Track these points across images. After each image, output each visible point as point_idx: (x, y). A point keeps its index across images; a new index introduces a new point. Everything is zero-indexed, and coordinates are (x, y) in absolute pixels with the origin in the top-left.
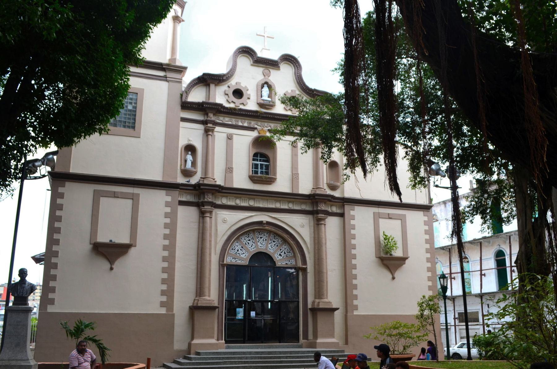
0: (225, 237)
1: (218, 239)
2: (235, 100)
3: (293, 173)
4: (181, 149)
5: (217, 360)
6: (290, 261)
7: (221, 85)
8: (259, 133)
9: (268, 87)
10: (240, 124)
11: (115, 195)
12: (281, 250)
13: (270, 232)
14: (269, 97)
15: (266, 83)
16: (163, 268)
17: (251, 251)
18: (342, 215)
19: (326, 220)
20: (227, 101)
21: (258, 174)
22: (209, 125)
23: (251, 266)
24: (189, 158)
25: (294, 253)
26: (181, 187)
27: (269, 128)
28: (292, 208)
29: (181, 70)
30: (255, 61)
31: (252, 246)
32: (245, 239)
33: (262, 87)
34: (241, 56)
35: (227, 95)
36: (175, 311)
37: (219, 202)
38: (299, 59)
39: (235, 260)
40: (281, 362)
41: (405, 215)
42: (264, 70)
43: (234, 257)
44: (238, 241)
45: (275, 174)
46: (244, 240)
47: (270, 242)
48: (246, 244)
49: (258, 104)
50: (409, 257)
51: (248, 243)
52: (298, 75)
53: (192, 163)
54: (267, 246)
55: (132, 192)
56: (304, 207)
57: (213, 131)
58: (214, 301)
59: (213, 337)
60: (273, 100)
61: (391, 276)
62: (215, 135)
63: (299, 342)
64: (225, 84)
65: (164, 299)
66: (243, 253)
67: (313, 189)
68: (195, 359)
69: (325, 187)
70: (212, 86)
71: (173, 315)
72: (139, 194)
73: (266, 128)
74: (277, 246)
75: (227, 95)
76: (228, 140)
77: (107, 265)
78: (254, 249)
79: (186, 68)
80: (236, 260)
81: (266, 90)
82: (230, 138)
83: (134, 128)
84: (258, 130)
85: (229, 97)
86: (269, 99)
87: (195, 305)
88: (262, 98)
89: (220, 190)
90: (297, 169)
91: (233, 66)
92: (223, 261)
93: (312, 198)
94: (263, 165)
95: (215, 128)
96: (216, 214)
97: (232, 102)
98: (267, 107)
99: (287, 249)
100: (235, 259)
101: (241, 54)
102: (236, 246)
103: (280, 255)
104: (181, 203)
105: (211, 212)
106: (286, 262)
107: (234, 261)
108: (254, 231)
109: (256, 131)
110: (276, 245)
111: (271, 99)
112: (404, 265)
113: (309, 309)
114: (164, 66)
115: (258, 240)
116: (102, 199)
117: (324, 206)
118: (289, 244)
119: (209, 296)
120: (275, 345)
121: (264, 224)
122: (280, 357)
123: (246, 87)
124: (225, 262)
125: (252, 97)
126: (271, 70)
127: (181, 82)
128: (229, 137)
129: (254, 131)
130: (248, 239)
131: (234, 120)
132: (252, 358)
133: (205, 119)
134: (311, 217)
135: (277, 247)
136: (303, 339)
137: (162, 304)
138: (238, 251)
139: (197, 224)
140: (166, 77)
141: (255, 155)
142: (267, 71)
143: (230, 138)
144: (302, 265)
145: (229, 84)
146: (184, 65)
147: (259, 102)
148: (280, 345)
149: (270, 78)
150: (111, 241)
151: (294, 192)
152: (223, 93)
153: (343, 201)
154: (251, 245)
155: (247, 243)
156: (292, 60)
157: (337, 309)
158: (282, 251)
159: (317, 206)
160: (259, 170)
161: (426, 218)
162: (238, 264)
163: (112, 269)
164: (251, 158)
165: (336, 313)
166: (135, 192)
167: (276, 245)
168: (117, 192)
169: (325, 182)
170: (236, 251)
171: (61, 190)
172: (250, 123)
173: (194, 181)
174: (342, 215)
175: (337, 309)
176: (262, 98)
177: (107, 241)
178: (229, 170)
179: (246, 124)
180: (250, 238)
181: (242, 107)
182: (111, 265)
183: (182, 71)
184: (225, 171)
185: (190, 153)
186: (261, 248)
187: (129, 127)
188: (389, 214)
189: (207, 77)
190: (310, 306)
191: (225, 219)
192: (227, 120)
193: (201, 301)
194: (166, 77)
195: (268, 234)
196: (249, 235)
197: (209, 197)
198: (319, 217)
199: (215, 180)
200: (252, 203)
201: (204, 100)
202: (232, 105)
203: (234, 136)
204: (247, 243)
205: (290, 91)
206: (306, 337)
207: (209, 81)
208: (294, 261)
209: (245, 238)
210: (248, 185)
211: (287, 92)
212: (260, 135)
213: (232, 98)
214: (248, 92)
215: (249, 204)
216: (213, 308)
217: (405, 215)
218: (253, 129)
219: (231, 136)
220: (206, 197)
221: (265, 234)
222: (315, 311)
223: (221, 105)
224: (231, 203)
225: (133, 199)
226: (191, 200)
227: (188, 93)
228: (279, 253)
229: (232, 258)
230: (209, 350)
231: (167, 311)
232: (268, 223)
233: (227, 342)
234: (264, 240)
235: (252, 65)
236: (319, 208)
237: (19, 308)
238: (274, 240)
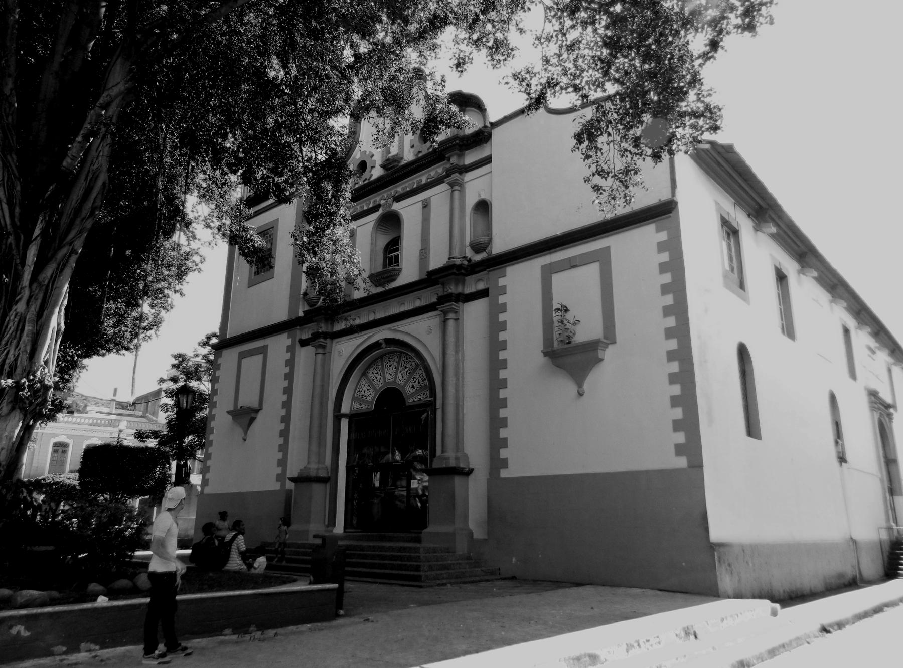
103: (413, 387)
106: (420, 397)
161: (663, 236)
228: (411, 384)
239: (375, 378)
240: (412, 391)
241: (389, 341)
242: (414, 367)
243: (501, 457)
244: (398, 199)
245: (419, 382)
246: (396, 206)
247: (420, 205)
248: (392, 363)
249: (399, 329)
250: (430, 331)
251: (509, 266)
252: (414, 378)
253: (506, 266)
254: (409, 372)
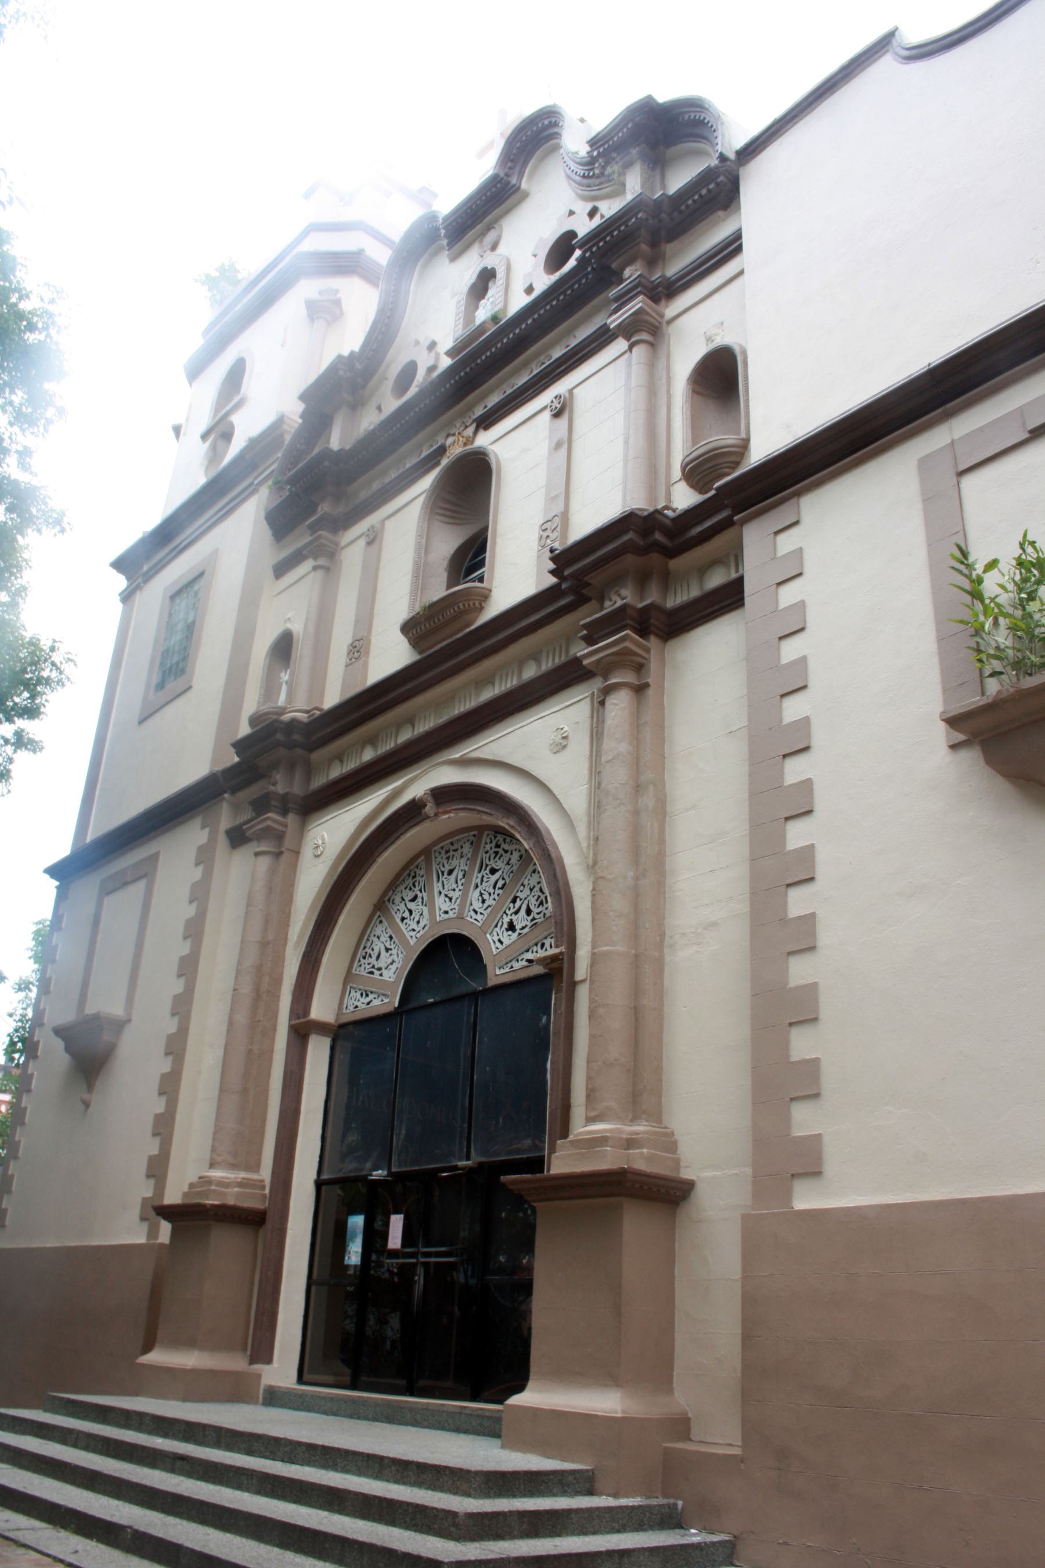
31: (418, 922)
39: (368, 1000)
51: (411, 912)
80: (371, 997)
103: (511, 927)
186: (446, 916)
228: (506, 920)
235: (453, 259)
239: (407, 914)
240: (509, 938)
241: (444, 795)
242: (515, 868)
244: (486, 422)
245: (529, 912)
246: (484, 440)
247: (547, 415)
248: (454, 863)
249: (474, 755)
250: (561, 745)
251: (809, 489)
252: (514, 901)
253: (799, 494)
254: (499, 885)
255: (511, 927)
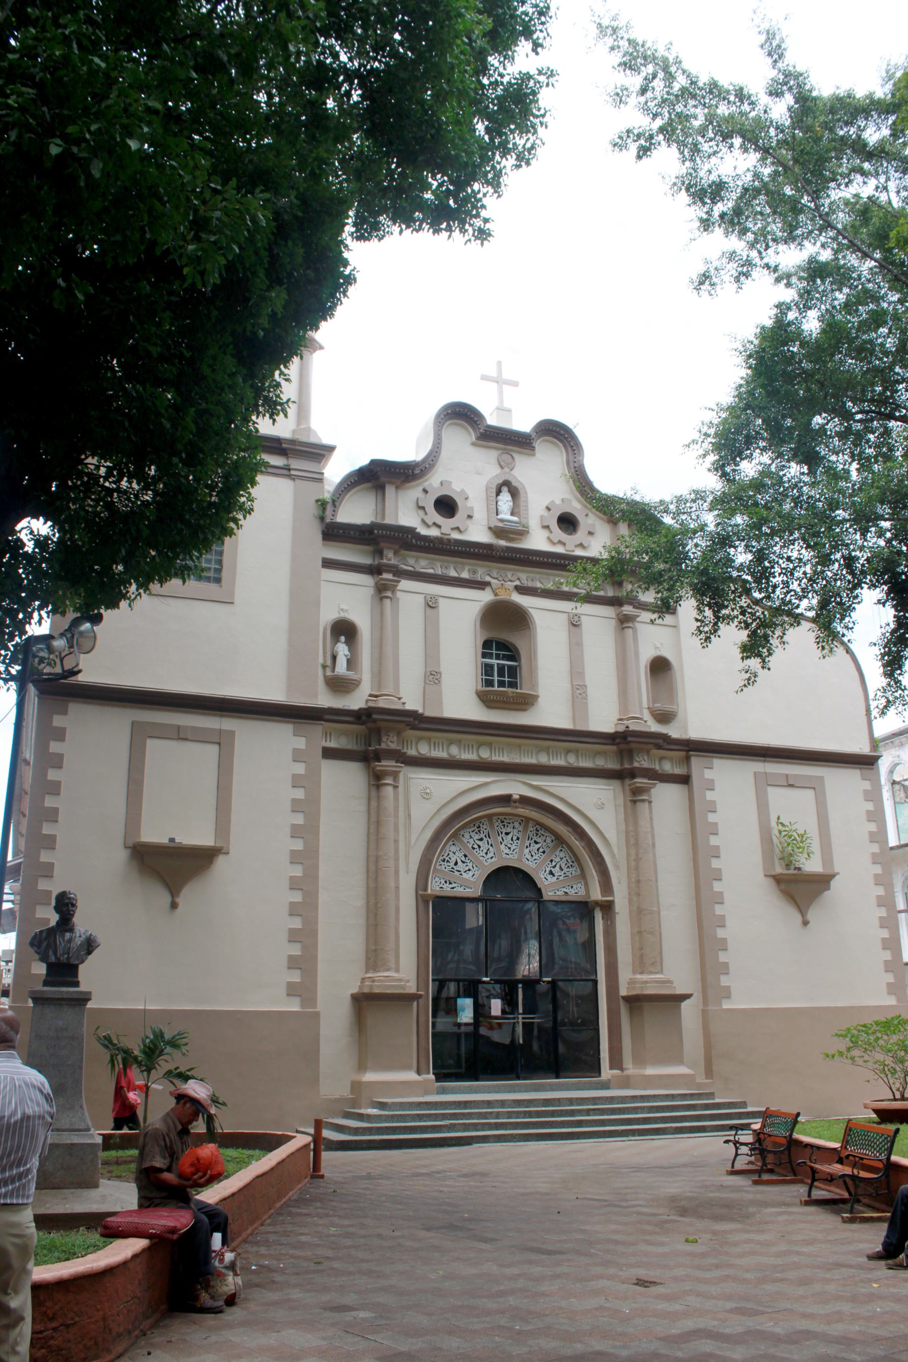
0: (429, 834)
1: (414, 838)
2: (440, 520)
3: (575, 683)
4: (325, 629)
5: (430, 1121)
6: (575, 887)
7: (409, 488)
8: (496, 595)
9: (509, 491)
10: (453, 573)
11: (180, 735)
12: (551, 861)
13: (526, 821)
14: (512, 514)
15: (506, 483)
16: (292, 904)
17: (486, 864)
18: (685, 780)
19: (652, 790)
20: (423, 522)
21: (493, 686)
22: (386, 576)
23: (486, 900)
24: (342, 649)
25: (582, 870)
26: (326, 717)
27: (517, 583)
28: (576, 764)
29: (320, 453)
30: (481, 434)
31: (486, 853)
32: (471, 837)
33: (498, 492)
34: (450, 424)
35: (423, 508)
36: (321, 1006)
37: (412, 752)
38: (578, 432)
40: (579, 1124)
41: (823, 777)
42: (501, 455)
43: (447, 879)
44: (456, 842)
45: (534, 685)
46: (470, 838)
47: (527, 843)
48: (474, 848)
49: (490, 528)
50: (838, 874)
51: (479, 847)
52: (576, 465)
53: (348, 661)
54: (521, 853)
55: (217, 726)
56: (601, 763)
57: (393, 589)
58: (408, 981)
59: (406, 1067)
60: (524, 521)
61: (799, 918)
62: (398, 599)
63: (600, 1075)
64: (418, 485)
65: (296, 977)
66: (467, 868)
67: (621, 720)
68: (379, 1118)
69: (647, 716)
70: (390, 491)
71: (317, 1015)
72: (232, 733)
73: (509, 583)
74: (544, 852)
75: (423, 508)
76: (428, 609)
77: (166, 899)
78: (493, 860)
79: (331, 449)
81: (505, 499)
82: (431, 605)
83: (218, 580)
84: (494, 587)
85: (426, 514)
86: (515, 519)
87: (366, 990)
88: (500, 517)
89: (417, 722)
90: (582, 674)
91: (434, 445)
92: (426, 889)
93: (618, 741)
94: (503, 666)
95: (399, 582)
96: (407, 780)
97: (435, 524)
98: (511, 536)
99: (564, 859)
100: (450, 883)
101: (450, 419)
102: (451, 853)
103: (551, 873)
104: (329, 754)
105: (395, 775)
106: (565, 890)
107: (447, 887)
108: (490, 817)
109: (488, 589)
110: (541, 850)
111: (519, 518)
112: (827, 893)
113: (623, 998)
114: (284, 445)
115: (500, 839)
116: (151, 744)
117: (646, 758)
118: (570, 848)
119: (397, 970)
120: (550, 1084)
121: (515, 802)
122: (572, 1113)
123: (463, 491)
124: (429, 891)
125: (476, 516)
126: (515, 455)
127: (320, 480)
128: (430, 604)
129: (483, 589)
130: (477, 837)
131: (439, 564)
132: (510, 1115)
133: (376, 562)
134: (615, 785)
135: (544, 856)
136: (611, 1068)
137: (292, 990)
138: (456, 864)
139: (364, 802)
140: (289, 470)
141: (487, 644)
142: (506, 457)
143: (431, 605)
144: (603, 896)
145: (426, 485)
146: (326, 440)
147: (493, 526)
148: (559, 1083)
149: (515, 472)
150: (172, 840)
151: (578, 728)
152: (414, 505)
153: (687, 748)
154: (485, 851)
155: (476, 846)
156: (561, 435)
157: (687, 996)
158: (554, 864)
159: (631, 760)
160: (496, 678)
161: (867, 785)
162: (458, 895)
163: (174, 906)
164: (480, 651)
165: (685, 1005)
166: (224, 727)
167: (541, 850)
168: (186, 727)
169: (645, 705)
170: (452, 864)
171: (58, 721)
172: (475, 572)
173: (356, 701)
174: (685, 780)
175: (687, 996)
176: (500, 517)
177: (164, 840)
178: (433, 677)
179: (465, 575)
180: (482, 836)
181: (455, 536)
182: (173, 896)
183: (323, 456)
184: (423, 679)
185: (343, 638)
187: (208, 579)
188: (787, 775)
189: (378, 469)
190: (623, 992)
191: (428, 791)
192: (423, 564)
193: (379, 981)
194: (289, 470)
195: (523, 824)
196: (479, 827)
197: (390, 738)
198: (638, 785)
199: (402, 701)
200: (485, 754)
201: (374, 520)
202: (434, 532)
203: (441, 600)
204: (476, 846)
205: (558, 502)
206: (617, 1063)
207: (383, 479)
208: (583, 887)
209: (473, 834)
210: (474, 712)
211: (553, 502)
212: (498, 597)
213: (434, 516)
214: (469, 504)
215: (479, 756)
216: (406, 999)
217: (823, 777)
218: (481, 585)
219: (433, 600)
220: (384, 739)
221: (516, 825)
222: (635, 1002)
223: (411, 531)
224: (439, 753)
225: (219, 744)
226: (349, 747)
227: (337, 504)
228: (548, 870)
229: (443, 881)
230: (403, 1097)
231: (302, 1007)
232: (525, 801)
233: (440, 1077)
234: (515, 838)
235: (473, 444)
236: (636, 765)
237: (61, 992)
238: (535, 838)
243: (722, 984)
245: (561, 869)
255: (551, 873)
